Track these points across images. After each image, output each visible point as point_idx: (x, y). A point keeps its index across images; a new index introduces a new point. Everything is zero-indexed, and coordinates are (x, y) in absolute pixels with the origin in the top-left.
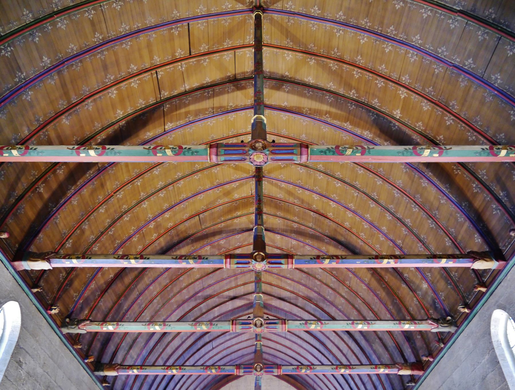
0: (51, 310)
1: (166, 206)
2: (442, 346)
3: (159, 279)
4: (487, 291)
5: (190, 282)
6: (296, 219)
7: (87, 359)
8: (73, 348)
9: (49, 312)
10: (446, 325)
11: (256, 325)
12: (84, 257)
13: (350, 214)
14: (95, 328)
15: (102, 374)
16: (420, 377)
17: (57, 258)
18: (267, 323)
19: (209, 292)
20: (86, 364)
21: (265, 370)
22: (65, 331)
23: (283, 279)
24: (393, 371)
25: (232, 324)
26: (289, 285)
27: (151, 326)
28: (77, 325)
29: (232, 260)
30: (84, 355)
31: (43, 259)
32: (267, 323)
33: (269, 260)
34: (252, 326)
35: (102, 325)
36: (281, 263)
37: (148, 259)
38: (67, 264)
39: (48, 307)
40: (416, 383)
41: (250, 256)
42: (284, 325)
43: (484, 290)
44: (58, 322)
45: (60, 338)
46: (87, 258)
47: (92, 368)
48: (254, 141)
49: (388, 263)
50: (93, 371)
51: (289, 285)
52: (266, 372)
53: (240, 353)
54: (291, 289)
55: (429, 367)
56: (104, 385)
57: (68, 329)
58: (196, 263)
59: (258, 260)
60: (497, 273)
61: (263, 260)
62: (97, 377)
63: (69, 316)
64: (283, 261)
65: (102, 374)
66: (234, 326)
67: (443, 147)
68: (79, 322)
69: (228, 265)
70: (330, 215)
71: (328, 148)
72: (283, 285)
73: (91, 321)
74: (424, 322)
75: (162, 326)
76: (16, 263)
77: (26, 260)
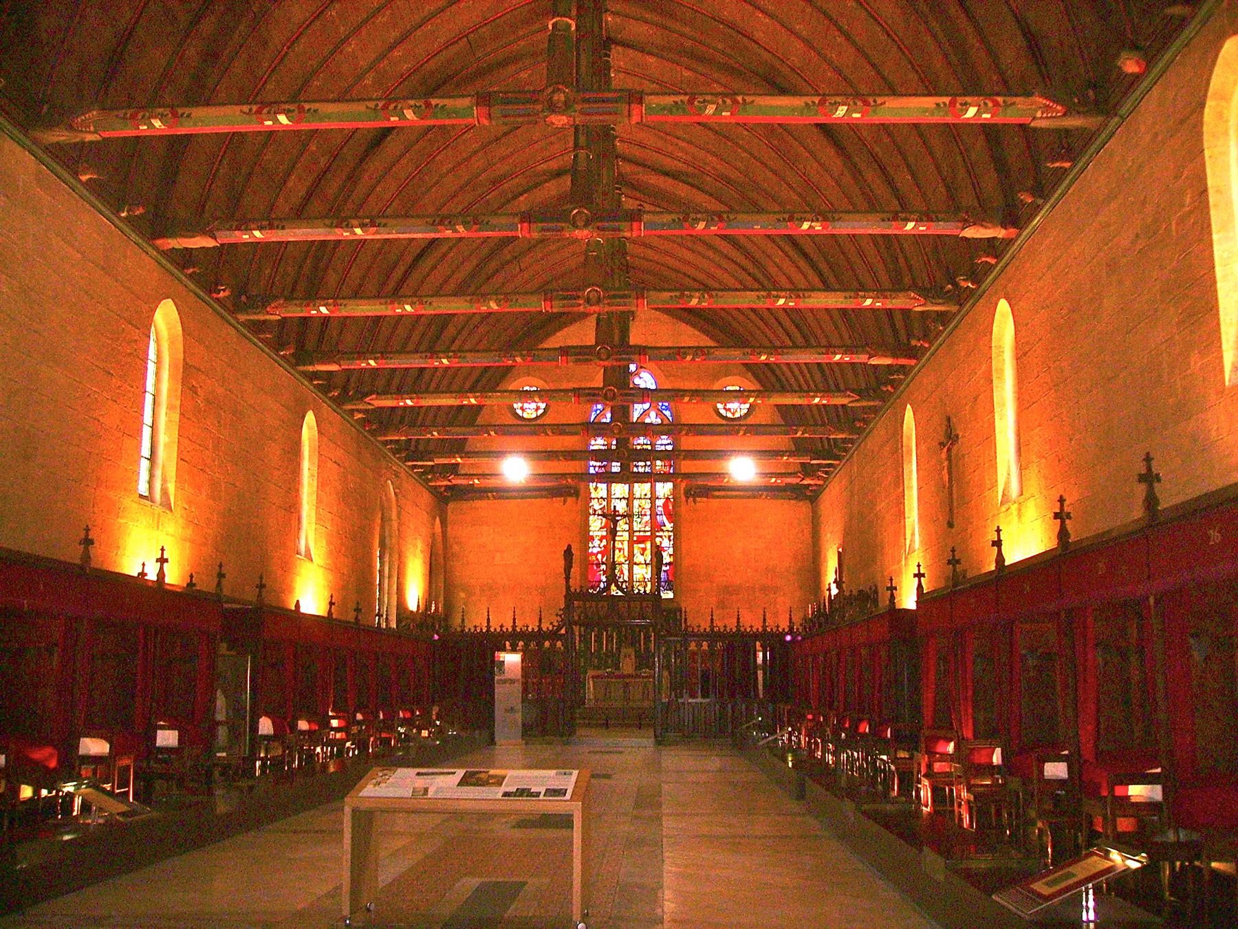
1: (395, 34)
4: (997, 263)
6: (687, 30)
8: (259, 339)
9: (215, 296)
11: (588, 301)
12: (271, 227)
13: (798, 45)
14: (295, 311)
15: (310, 368)
16: (913, 367)
19: (504, 168)
22: (243, 317)
24: (861, 358)
29: (533, 226)
30: (277, 345)
37: (385, 225)
39: (211, 289)
40: (906, 375)
41: (563, 217)
43: (993, 261)
44: (229, 305)
48: (550, 89)
50: (293, 366)
51: (682, 150)
55: (923, 354)
59: (580, 224)
60: (1009, 242)
61: (586, 226)
62: (304, 374)
64: (623, 225)
65: (310, 368)
67: (871, 100)
68: (264, 302)
70: (759, 35)
71: (676, 103)
76: (159, 242)
77: (173, 235)
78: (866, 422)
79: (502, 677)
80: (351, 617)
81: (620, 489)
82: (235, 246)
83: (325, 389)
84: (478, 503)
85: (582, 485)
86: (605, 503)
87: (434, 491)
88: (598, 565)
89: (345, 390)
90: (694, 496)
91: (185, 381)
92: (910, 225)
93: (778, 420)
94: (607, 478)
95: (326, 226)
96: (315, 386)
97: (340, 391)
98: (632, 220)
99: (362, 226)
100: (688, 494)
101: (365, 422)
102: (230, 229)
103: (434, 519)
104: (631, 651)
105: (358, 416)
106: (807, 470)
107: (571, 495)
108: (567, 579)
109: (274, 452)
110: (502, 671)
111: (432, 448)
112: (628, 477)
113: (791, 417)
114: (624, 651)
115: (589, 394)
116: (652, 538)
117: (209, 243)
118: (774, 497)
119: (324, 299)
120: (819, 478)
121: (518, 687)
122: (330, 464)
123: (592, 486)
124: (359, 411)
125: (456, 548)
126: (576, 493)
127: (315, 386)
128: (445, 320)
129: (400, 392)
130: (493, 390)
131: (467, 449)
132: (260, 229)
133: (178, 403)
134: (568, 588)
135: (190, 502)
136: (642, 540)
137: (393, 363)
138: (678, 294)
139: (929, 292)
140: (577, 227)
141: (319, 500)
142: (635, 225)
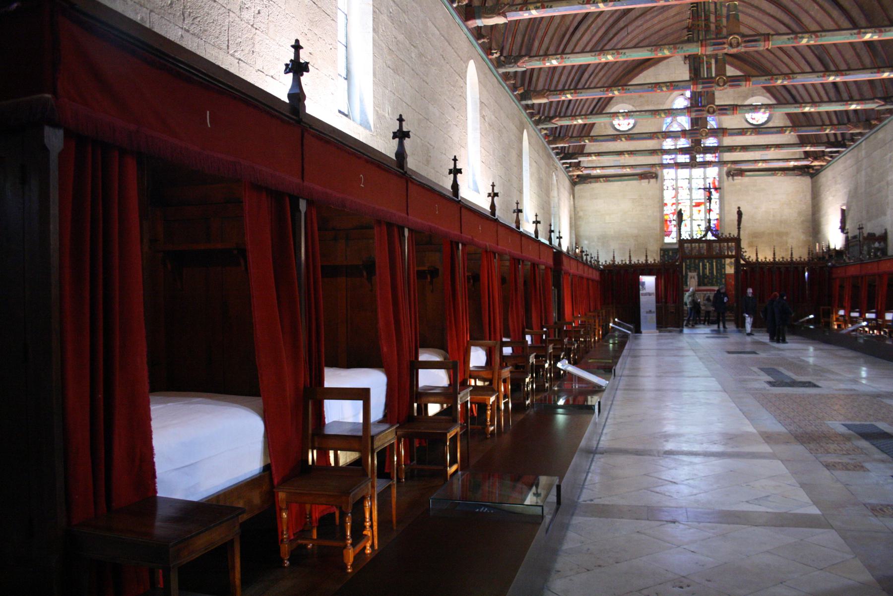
0: (492, 54)
9: (490, 57)
11: (731, 45)
12: (543, 7)
15: (529, 102)
20: (515, 96)
22: (501, 71)
25: (702, 46)
27: (602, 56)
28: (516, 62)
31: (499, 14)
32: (745, 42)
34: (726, 46)
35: (544, 60)
38: (525, 15)
42: (767, 43)
52: (730, 86)
53: (662, 33)
65: (529, 102)
73: (530, 57)
75: (616, 56)
77: (480, 18)
78: (880, 120)
79: (644, 292)
81: (684, 173)
82: (517, 22)
83: (531, 115)
86: (674, 183)
88: (670, 221)
90: (733, 176)
93: (789, 123)
94: (679, 165)
97: (540, 116)
100: (729, 174)
102: (516, 11)
104: (695, 274)
105: (544, 132)
106: (816, 156)
107: (653, 178)
110: (644, 288)
111: (570, 151)
113: (796, 121)
114: (690, 274)
118: (785, 175)
121: (653, 298)
122: (534, 164)
123: (665, 171)
124: (546, 129)
125: (581, 214)
126: (656, 177)
128: (583, 68)
129: (574, 116)
130: (601, 113)
131: (585, 151)
132: (537, 8)
133: (479, 126)
136: (698, 205)
138: (792, 36)
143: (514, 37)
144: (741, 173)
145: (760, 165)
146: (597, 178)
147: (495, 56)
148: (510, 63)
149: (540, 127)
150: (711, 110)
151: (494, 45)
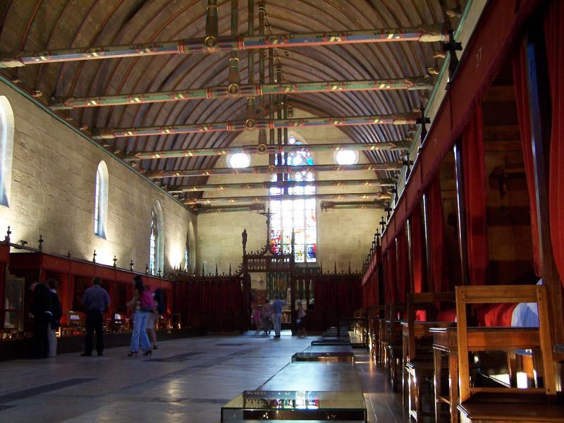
0: (36, 94)
2: (427, 101)
3: (142, 33)
5: (180, 27)
7: (82, 127)
9: (35, 96)
10: (422, 84)
11: (231, 91)
14: (80, 105)
15: (99, 138)
17: (27, 56)
18: (242, 89)
21: (256, 125)
22: (54, 108)
23: (293, 13)
24: (390, 122)
26: (300, 18)
28: (63, 102)
30: (78, 124)
32: (242, 89)
33: (221, 44)
36: (232, 47)
37: (109, 51)
41: (201, 41)
42: (258, 90)
44: (45, 102)
45: (51, 115)
46: (53, 55)
47: (90, 134)
49: (335, 40)
50: (90, 137)
51: (300, 18)
54: (305, 23)
56: (105, 146)
57: (55, 106)
58: (152, 51)
59: (210, 44)
61: (214, 44)
62: (97, 141)
63: (53, 95)
64: (233, 44)
65: (99, 138)
66: (210, 94)
68: (63, 100)
69: (182, 52)
72: (294, 18)
73: (75, 98)
74: (400, 81)
80: (128, 268)
84: (213, 214)
85: (267, 202)
87: (188, 207)
88: (276, 245)
89: (125, 150)
91: (15, 140)
92: (391, 36)
95: (78, 52)
96: (105, 148)
97: (121, 152)
98: (238, 41)
99: (97, 51)
101: (141, 168)
103: (189, 222)
106: (384, 192)
108: (244, 247)
109: (79, 181)
112: (285, 196)
115: (251, 149)
116: (305, 230)
117: (19, 64)
118: (368, 207)
119: (93, 97)
120: (389, 195)
122: (116, 189)
125: (202, 238)
126: (264, 208)
127: (105, 148)
132: (45, 55)
134: (245, 252)
135: (21, 203)
137: (143, 134)
139: (415, 79)
140: (208, 45)
141: (110, 208)
142: (240, 43)
143: (75, 82)
144: (332, 205)
145: (339, 199)
146: (215, 209)
147: (38, 95)
148: (59, 102)
149: (127, 160)
150: (262, 148)
151: (42, 85)
